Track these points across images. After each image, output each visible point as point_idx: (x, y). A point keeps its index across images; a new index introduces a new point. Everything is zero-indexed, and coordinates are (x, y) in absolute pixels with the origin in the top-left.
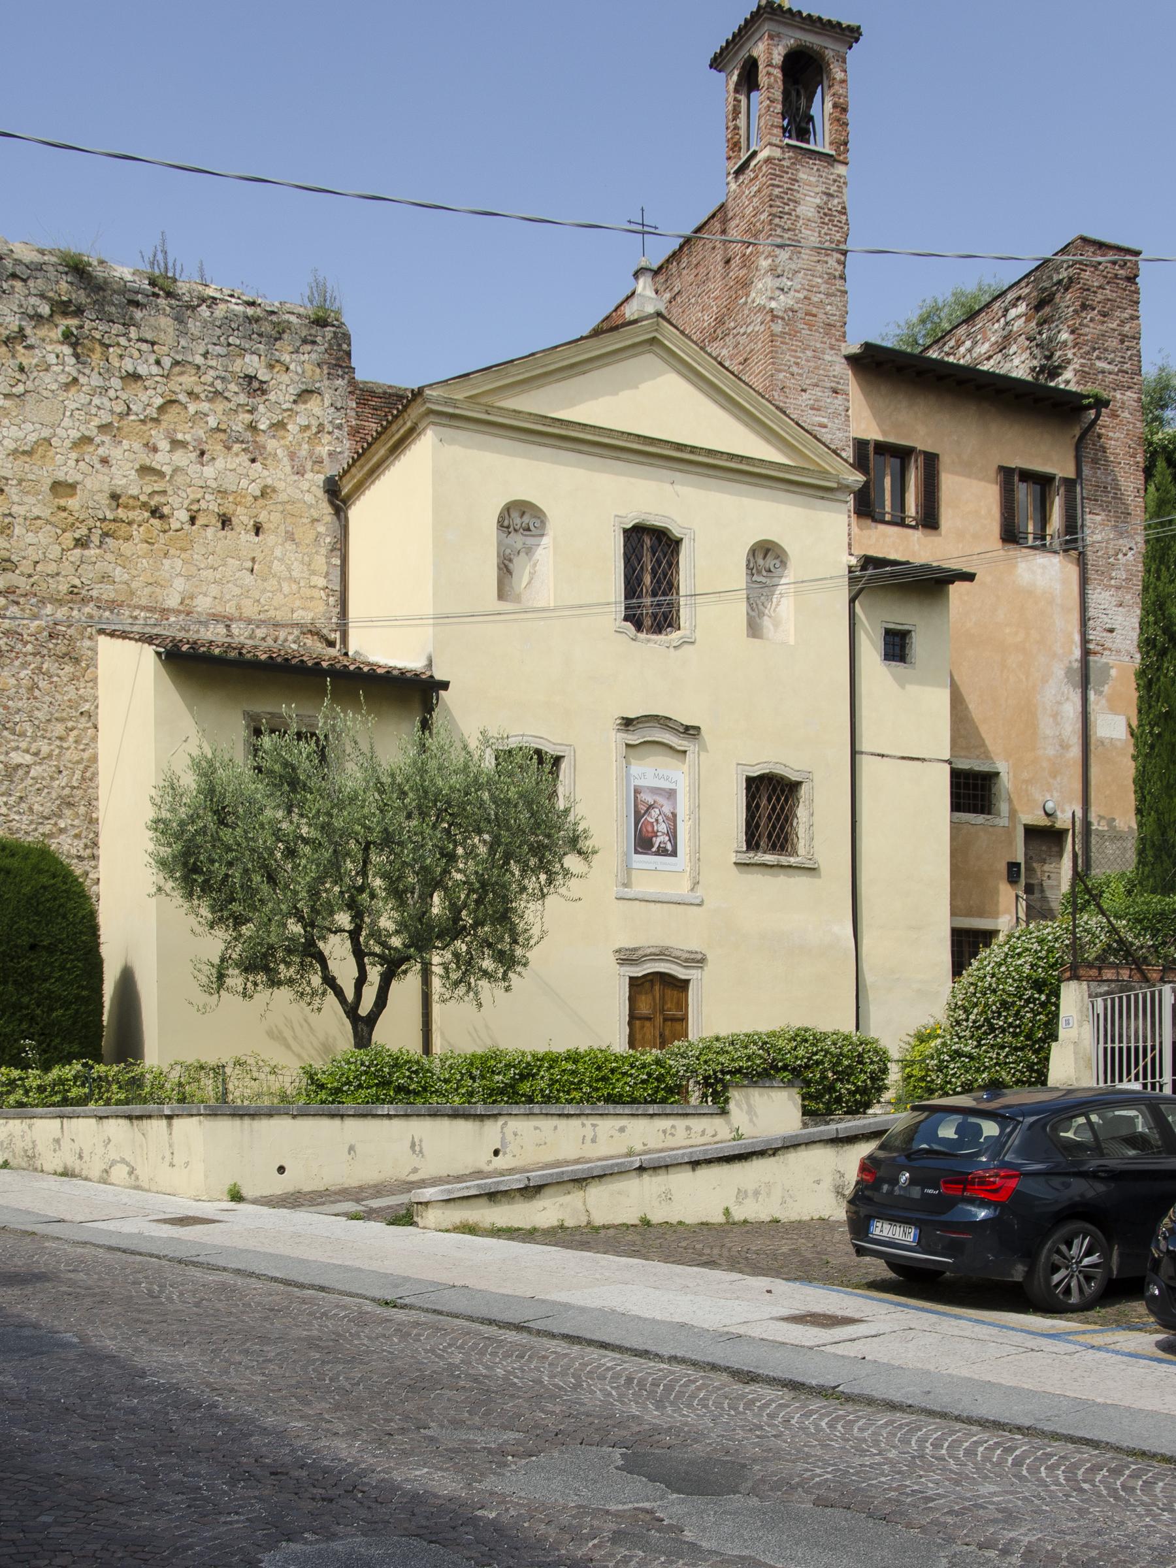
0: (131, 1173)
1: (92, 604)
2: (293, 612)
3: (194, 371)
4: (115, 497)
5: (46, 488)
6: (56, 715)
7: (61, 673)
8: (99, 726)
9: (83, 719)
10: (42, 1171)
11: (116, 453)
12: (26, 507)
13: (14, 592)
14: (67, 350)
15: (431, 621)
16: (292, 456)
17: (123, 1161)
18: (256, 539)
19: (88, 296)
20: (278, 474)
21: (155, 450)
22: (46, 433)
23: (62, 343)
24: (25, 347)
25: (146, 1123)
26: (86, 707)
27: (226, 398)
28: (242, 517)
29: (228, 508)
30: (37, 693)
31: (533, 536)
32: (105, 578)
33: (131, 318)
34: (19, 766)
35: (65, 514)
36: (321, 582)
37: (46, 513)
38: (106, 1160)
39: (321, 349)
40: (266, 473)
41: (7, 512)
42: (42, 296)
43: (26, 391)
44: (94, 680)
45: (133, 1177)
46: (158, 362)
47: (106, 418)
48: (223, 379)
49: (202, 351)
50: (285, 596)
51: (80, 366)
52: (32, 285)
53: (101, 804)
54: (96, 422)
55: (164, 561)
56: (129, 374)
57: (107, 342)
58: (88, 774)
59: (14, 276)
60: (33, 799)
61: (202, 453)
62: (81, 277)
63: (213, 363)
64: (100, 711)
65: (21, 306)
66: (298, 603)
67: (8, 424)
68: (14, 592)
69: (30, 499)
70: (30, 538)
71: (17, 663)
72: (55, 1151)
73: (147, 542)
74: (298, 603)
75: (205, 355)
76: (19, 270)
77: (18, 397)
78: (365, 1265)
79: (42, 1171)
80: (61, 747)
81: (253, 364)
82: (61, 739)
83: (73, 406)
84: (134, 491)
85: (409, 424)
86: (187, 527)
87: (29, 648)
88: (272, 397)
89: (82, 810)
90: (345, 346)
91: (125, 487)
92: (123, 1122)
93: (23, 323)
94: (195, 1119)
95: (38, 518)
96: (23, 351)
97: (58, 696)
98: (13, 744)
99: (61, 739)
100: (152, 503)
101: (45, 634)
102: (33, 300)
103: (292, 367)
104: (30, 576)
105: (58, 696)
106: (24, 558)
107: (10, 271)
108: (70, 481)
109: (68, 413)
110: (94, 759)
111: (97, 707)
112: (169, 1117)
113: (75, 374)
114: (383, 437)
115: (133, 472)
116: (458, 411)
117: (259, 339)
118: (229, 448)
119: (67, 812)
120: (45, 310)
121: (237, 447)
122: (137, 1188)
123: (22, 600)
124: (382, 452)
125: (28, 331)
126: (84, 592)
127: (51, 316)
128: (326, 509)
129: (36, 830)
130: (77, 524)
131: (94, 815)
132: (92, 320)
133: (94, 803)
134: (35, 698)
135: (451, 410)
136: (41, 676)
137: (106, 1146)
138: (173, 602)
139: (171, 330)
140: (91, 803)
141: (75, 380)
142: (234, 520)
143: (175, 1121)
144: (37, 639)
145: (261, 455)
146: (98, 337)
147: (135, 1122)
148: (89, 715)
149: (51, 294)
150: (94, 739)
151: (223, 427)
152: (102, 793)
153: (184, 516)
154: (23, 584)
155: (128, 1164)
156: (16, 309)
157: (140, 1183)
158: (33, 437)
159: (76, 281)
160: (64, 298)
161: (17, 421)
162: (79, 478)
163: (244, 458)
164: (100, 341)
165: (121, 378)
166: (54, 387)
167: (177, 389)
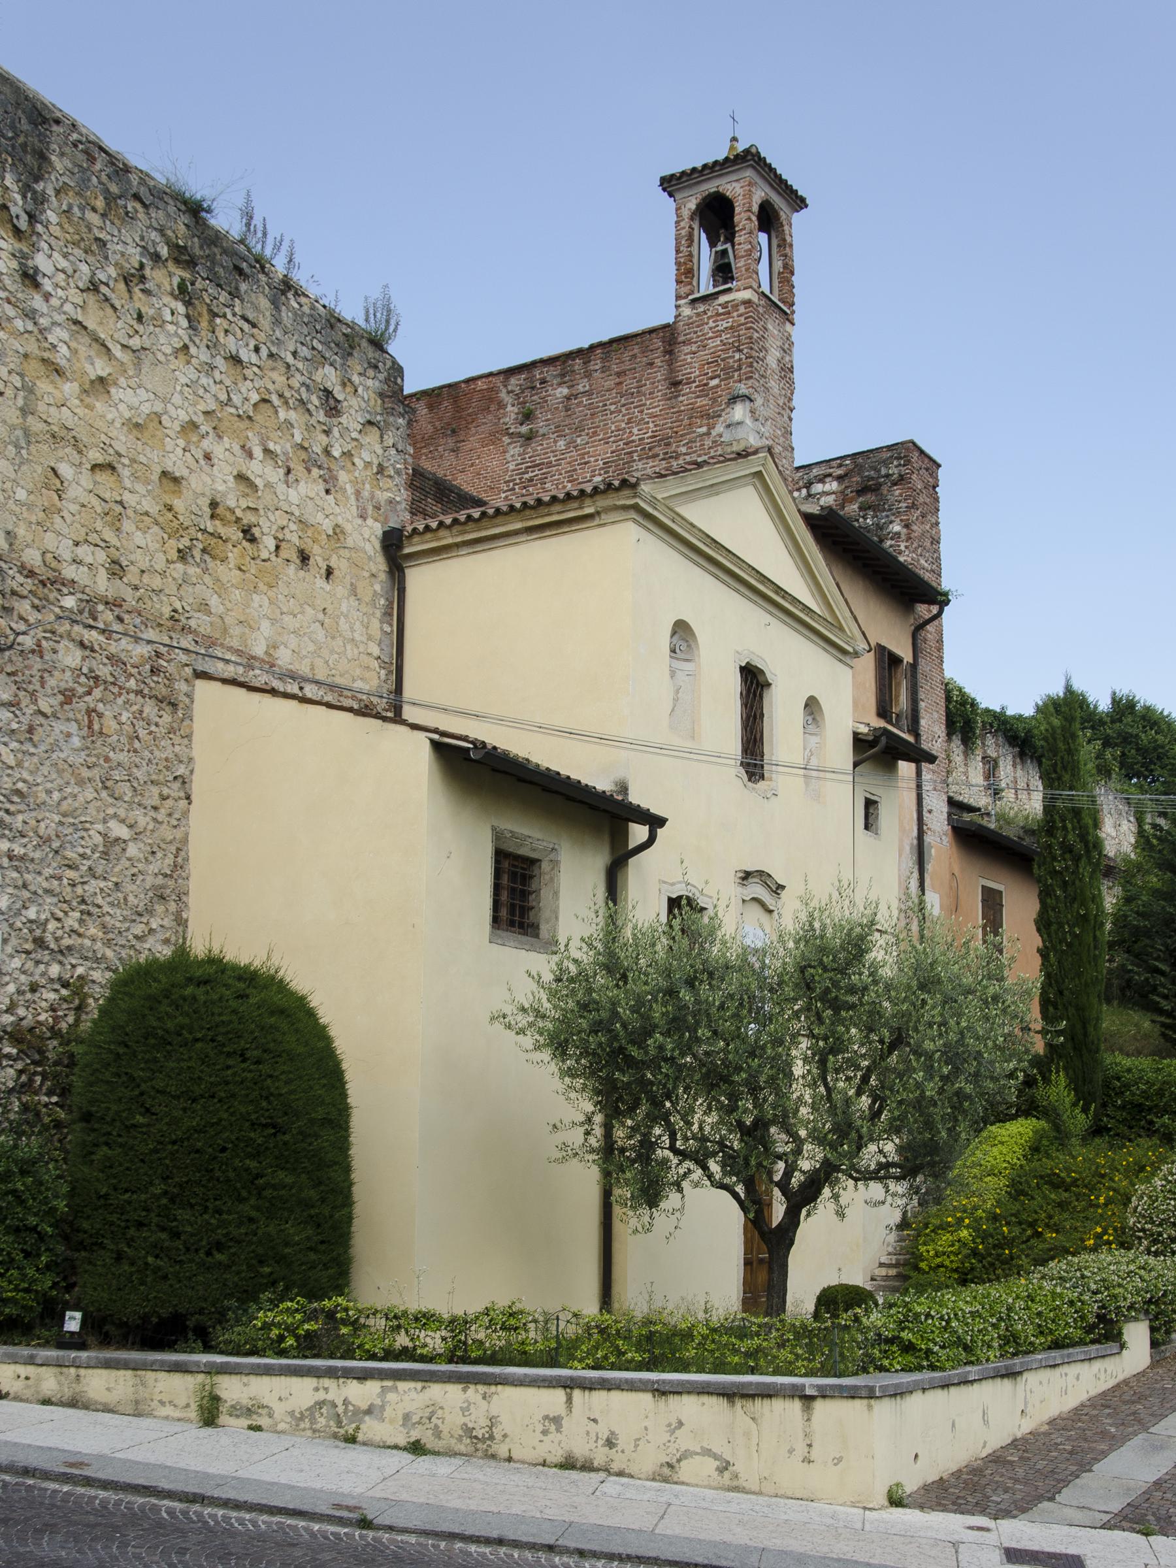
0: (722, 1470)
1: (190, 637)
2: (354, 681)
3: (283, 370)
4: (214, 505)
5: (155, 477)
6: (154, 777)
7: (160, 721)
8: (193, 797)
9: (177, 785)
10: (509, 1459)
11: (218, 451)
12: (136, 498)
13: (121, 606)
14: (181, 308)
15: (802, 772)
16: (358, 493)
17: (707, 1452)
18: (328, 588)
19: (201, 247)
20: (345, 514)
21: (250, 455)
22: (158, 407)
23: (176, 298)
24: (142, 290)
25: (761, 1407)
26: (181, 770)
27: (308, 410)
28: (318, 560)
29: (308, 545)
30: (137, 745)
31: (677, 659)
32: (204, 607)
33: (237, 289)
34: (117, 839)
35: (170, 515)
36: (376, 651)
37: (154, 509)
38: (672, 1450)
39: (381, 377)
40: (337, 510)
41: (118, 499)
42: (161, 231)
43: (144, 349)
44: (189, 736)
45: (727, 1474)
46: (257, 350)
47: (212, 405)
48: (308, 387)
49: (292, 349)
50: (349, 661)
51: (192, 332)
52: (153, 215)
53: (192, 900)
54: (202, 407)
55: (254, 596)
56: (232, 356)
57: (215, 310)
58: (179, 860)
59: (136, 197)
60: (129, 887)
61: (289, 471)
62: (197, 222)
63: (300, 365)
64: (194, 777)
65: (142, 238)
66: (358, 672)
67: (124, 385)
68: (121, 606)
69: (140, 488)
70: (139, 538)
71: (120, 701)
72: (545, 1432)
73: (240, 569)
74: (358, 672)
75: (295, 354)
76: (143, 191)
77: (134, 351)
78: (776, 1543)
79: (509, 1459)
80: (155, 820)
81: (328, 376)
82: (155, 808)
83: (184, 380)
84: (232, 503)
85: (589, 510)
86: (273, 558)
87: (132, 683)
88: (343, 419)
89: (173, 907)
90: (399, 381)
91: (224, 495)
92: (715, 1404)
93: (144, 261)
94: (857, 1402)
95: (147, 514)
96: (140, 294)
97: (157, 753)
98: (111, 811)
99: (155, 808)
100: (245, 521)
101: (148, 667)
102: (154, 235)
103: (360, 390)
104: (136, 588)
105: (157, 753)
106: (132, 563)
107: (135, 190)
108: (177, 474)
109: (178, 388)
110: (185, 840)
111: (192, 772)
112: (808, 1399)
113: (187, 341)
114: (528, 512)
115: (232, 479)
116: (655, 513)
117: (336, 350)
118: (309, 471)
119: (159, 908)
120: (164, 251)
121: (315, 472)
122: (736, 1489)
123: (126, 617)
124: (518, 526)
125: (147, 272)
126: (184, 621)
127: (166, 260)
128: (380, 564)
129: (128, 930)
130: (181, 532)
131: (185, 916)
132: (203, 279)
133: (184, 898)
134: (135, 751)
135: (650, 510)
136: (141, 723)
137: (672, 1432)
138: (259, 650)
139: (268, 314)
140: (181, 897)
141: (186, 347)
142: (312, 561)
143: (819, 1405)
144: (139, 673)
145: (335, 486)
146: (208, 301)
147: (739, 1403)
148: (183, 781)
149: (169, 233)
150: (186, 814)
151: (306, 445)
152: (193, 885)
153: (271, 544)
154: (129, 595)
155: (716, 1457)
156: (137, 239)
157: (741, 1482)
158: (146, 409)
159: (192, 225)
160: (181, 243)
161: (133, 385)
162: (185, 473)
163: (321, 487)
164: (208, 305)
165: (225, 358)
166: (169, 351)
167: (271, 387)
